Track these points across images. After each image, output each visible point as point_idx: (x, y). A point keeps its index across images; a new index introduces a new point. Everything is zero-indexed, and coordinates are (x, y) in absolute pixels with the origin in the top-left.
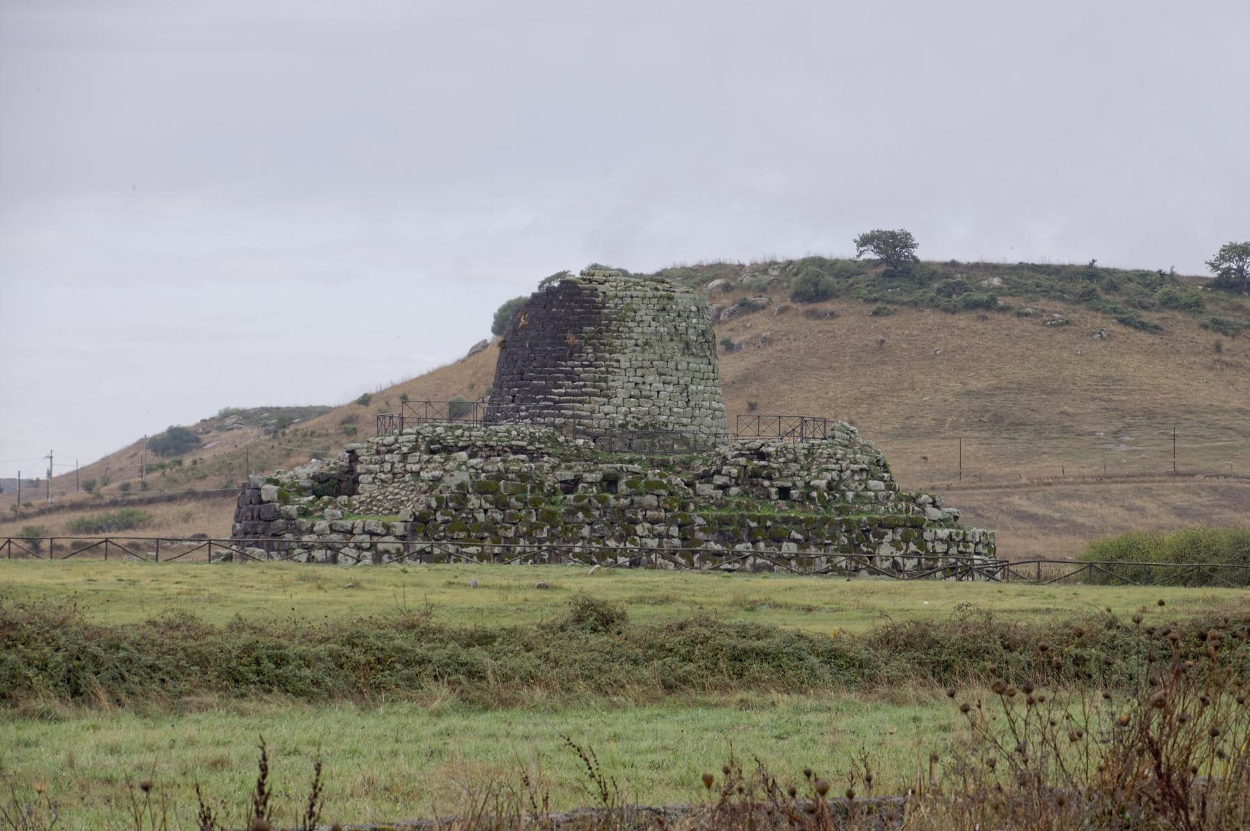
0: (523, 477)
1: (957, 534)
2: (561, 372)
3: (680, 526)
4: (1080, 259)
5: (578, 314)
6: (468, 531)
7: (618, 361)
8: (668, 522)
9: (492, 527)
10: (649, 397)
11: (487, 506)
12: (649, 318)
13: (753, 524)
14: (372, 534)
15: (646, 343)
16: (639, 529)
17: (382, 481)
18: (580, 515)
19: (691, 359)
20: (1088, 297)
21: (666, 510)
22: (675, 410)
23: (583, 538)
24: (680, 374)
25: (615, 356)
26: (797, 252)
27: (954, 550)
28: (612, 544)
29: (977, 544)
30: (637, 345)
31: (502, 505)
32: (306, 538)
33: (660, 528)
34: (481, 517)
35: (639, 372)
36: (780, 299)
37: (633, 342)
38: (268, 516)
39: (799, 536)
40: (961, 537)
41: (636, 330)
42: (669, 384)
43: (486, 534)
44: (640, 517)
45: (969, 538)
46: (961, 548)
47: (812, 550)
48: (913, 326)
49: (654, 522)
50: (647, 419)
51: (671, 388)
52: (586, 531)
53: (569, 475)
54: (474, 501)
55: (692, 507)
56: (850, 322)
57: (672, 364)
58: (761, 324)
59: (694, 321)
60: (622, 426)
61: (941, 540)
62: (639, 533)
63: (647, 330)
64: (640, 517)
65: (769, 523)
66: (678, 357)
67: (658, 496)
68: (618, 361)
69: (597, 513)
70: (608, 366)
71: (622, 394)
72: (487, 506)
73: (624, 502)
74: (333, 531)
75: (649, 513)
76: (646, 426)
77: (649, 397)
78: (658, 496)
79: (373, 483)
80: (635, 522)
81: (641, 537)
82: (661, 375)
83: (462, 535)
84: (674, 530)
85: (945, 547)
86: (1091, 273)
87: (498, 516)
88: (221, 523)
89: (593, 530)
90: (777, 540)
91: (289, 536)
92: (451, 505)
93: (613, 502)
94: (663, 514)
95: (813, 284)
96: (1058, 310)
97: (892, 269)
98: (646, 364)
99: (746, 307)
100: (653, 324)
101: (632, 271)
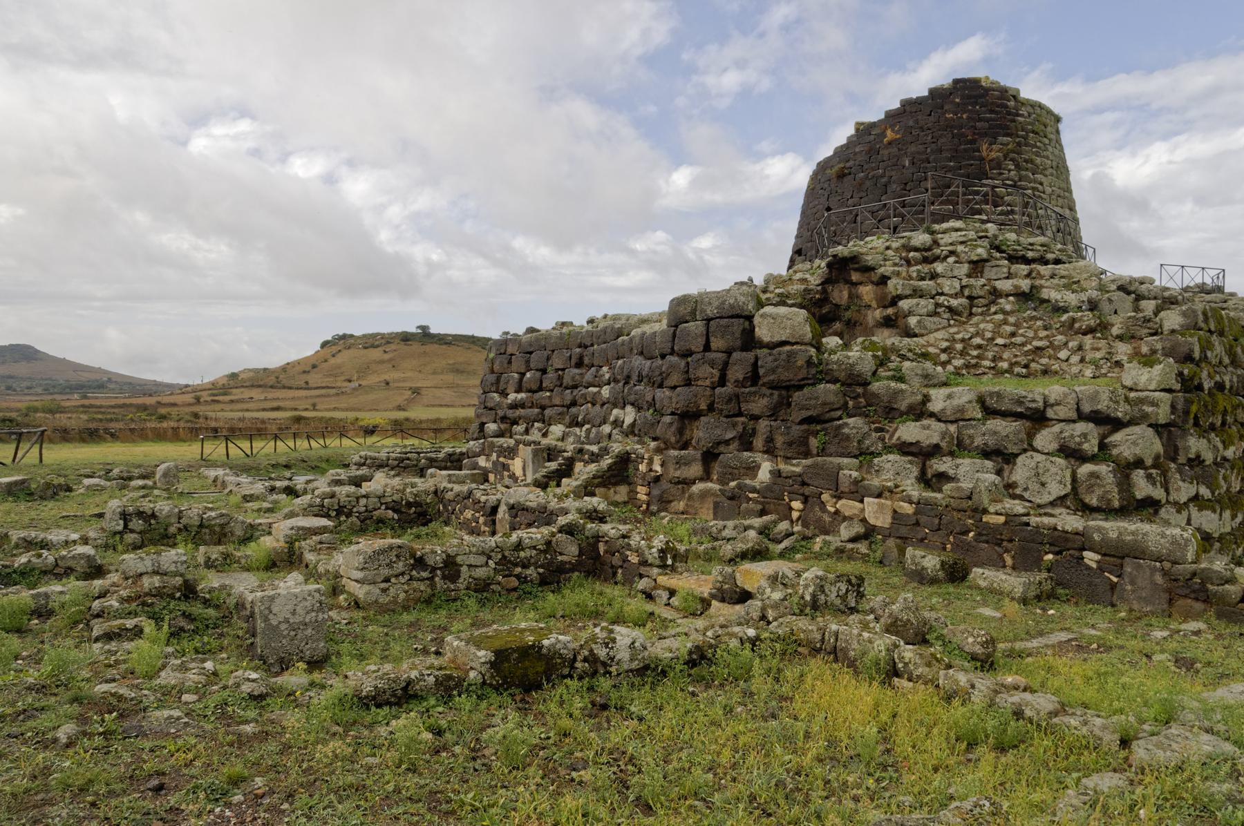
2: (977, 193)
4: (470, 333)
5: (988, 120)
14: (1097, 418)
17: (950, 309)
20: (473, 343)
25: (1039, 177)
26: (400, 330)
32: (909, 431)
36: (397, 341)
38: (785, 375)
48: (431, 348)
56: (416, 347)
58: (393, 347)
68: (1041, 184)
70: (1033, 189)
74: (990, 412)
79: (935, 314)
86: (473, 337)
88: (423, 392)
91: (854, 424)
95: (406, 338)
96: (467, 345)
97: (425, 335)
99: (389, 342)
101: (357, 333)
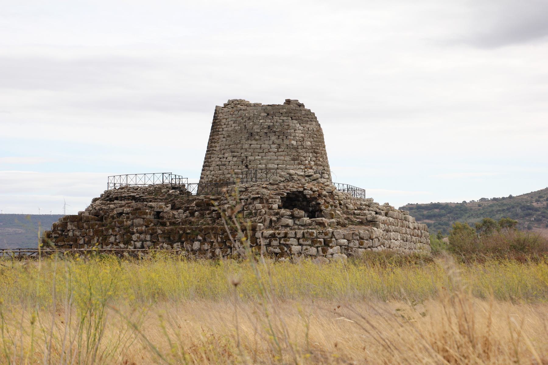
0: (106, 212)
1: (279, 234)
3: (151, 235)
6: (64, 241)
7: (216, 147)
8: (145, 233)
9: (75, 239)
10: (224, 165)
11: (74, 228)
12: (232, 122)
13: (181, 232)
15: (229, 136)
16: (134, 237)
18: (110, 231)
19: (254, 142)
21: (147, 226)
22: (236, 171)
23: (112, 243)
24: (242, 151)
27: (275, 243)
28: (122, 245)
29: (298, 239)
30: (224, 138)
31: (80, 228)
33: (142, 236)
34: (71, 234)
35: (222, 152)
37: (222, 136)
39: (200, 238)
40: (282, 235)
41: (225, 129)
42: (235, 157)
43: (71, 243)
44: (135, 230)
45: (289, 235)
46: (282, 242)
47: (206, 246)
49: (141, 233)
50: (222, 177)
51: (235, 159)
52: (112, 239)
53: (120, 210)
54: (69, 226)
55: (168, 224)
57: (239, 146)
59: (261, 121)
60: (211, 181)
61: (266, 238)
62: (134, 239)
63: (230, 129)
64: (135, 230)
65: (189, 231)
66: (244, 141)
67: (144, 219)
69: (117, 229)
71: (214, 164)
72: (74, 228)
73: (129, 223)
75: (139, 228)
76: (220, 180)
77: (224, 165)
78: (144, 219)
80: (133, 233)
81: (135, 241)
82: (232, 152)
83: (62, 243)
84: (148, 237)
85: (268, 241)
87: (77, 233)
89: (116, 239)
90: (193, 241)
92: (59, 228)
93: (125, 223)
94: (144, 228)
98: (227, 147)
100: (233, 125)
